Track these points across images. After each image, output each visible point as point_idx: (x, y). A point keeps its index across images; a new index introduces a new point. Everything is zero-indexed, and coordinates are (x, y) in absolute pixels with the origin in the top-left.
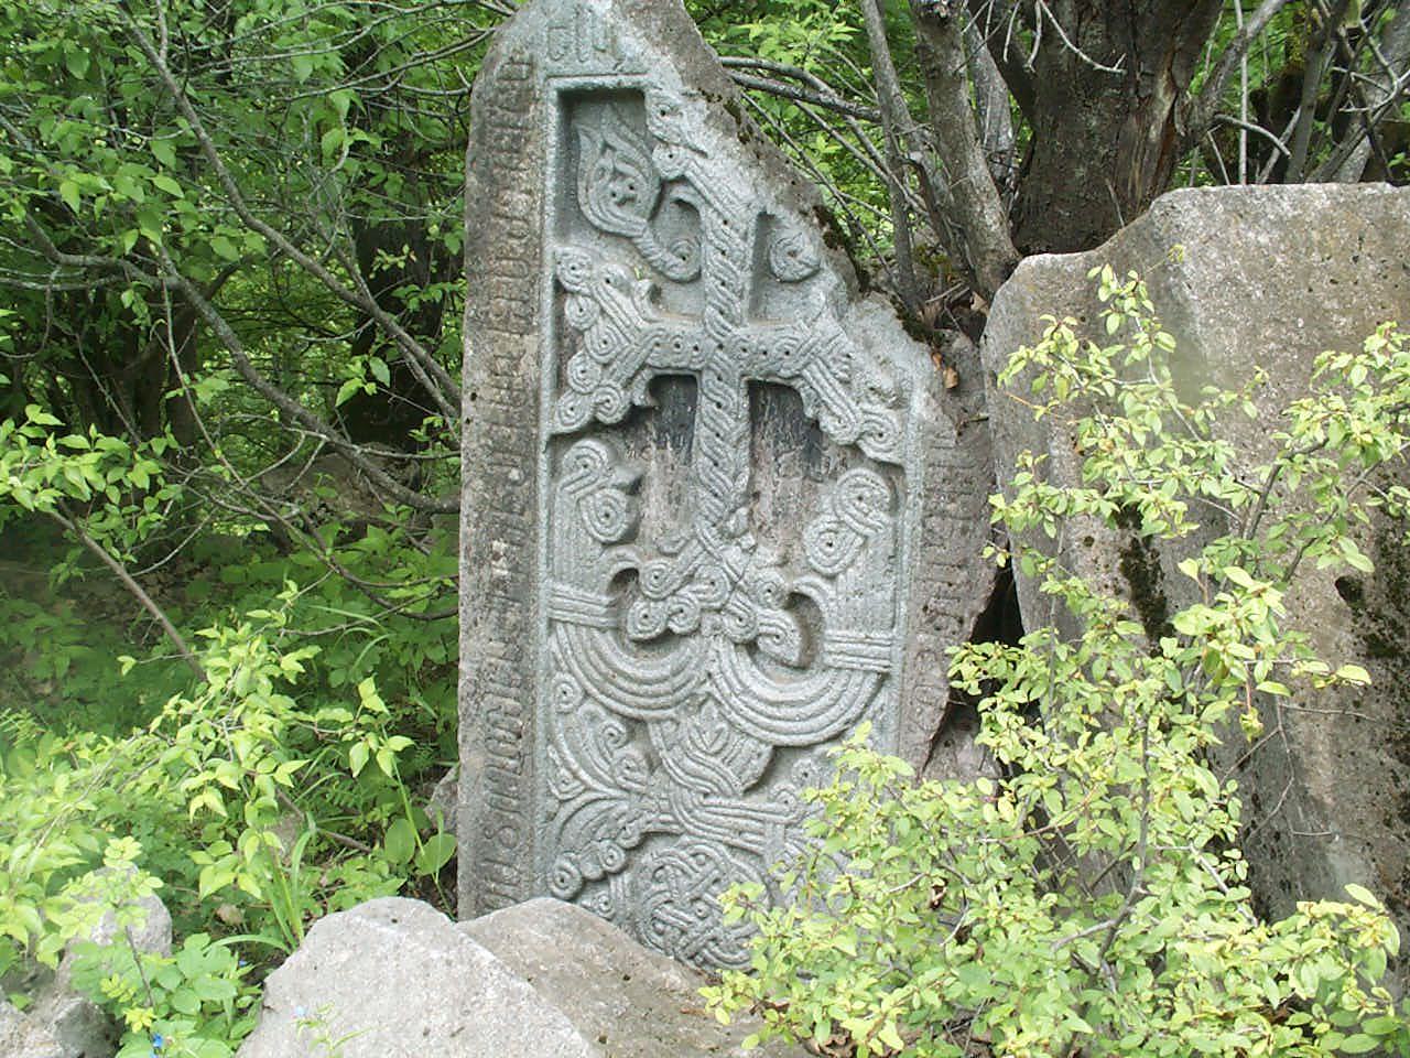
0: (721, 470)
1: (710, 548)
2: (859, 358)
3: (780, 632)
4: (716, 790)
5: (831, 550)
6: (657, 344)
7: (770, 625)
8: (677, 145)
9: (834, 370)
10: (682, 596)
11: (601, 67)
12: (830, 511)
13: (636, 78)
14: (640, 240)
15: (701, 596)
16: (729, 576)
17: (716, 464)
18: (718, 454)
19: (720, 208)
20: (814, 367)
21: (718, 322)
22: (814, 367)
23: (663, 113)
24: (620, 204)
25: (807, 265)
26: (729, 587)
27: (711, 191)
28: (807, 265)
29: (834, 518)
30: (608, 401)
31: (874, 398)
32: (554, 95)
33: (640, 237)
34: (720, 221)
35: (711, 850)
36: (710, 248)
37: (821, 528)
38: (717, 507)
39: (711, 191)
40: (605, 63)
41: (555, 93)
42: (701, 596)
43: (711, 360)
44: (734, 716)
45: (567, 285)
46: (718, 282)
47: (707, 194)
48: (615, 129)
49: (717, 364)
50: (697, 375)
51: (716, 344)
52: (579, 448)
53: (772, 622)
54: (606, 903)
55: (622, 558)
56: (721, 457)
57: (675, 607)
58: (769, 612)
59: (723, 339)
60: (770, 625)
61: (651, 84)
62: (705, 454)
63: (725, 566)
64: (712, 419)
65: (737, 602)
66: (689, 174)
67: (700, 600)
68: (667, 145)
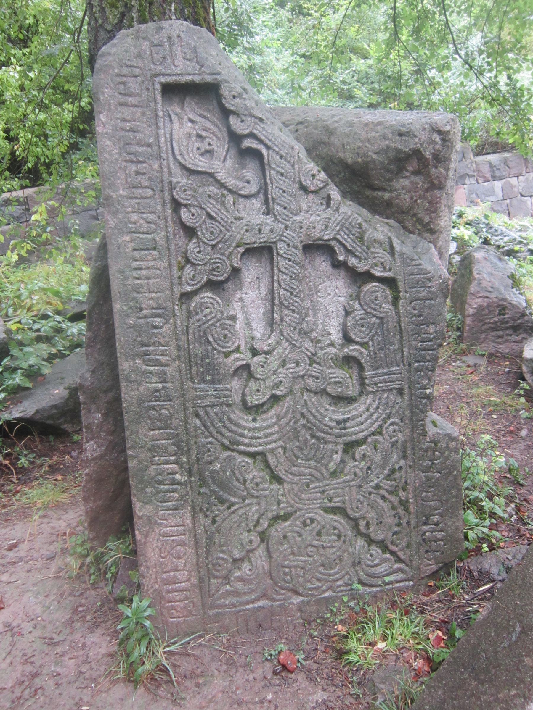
0: (295, 296)
1: (294, 342)
2: (365, 225)
3: (341, 380)
4: (313, 479)
5: (364, 329)
6: (247, 231)
7: (335, 378)
8: (245, 115)
9: (353, 232)
10: (280, 373)
11: (190, 70)
12: (360, 308)
13: (215, 77)
14: (219, 174)
15: (291, 370)
16: (307, 355)
17: (292, 293)
18: (292, 288)
19: (277, 149)
20: (342, 233)
21: (284, 214)
22: (342, 233)
23: (234, 97)
24: (202, 155)
25: (323, 182)
26: (308, 362)
27: (270, 140)
28: (323, 182)
29: (363, 311)
30: (218, 267)
31: (376, 245)
32: (158, 87)
33: (219, 172)
34: (278, 157)
35: (312, 514)
36: (273, 172)
37: (357, 318)
38: (295, 318)
39: (270, 140)
40: (192, 67)
41: (159, 85)
42: (291, 370)
43: (282, 236)
44: (319, 434)
45: (182, 201)
46: (281, 191)
47: (267, 142)
48: (193, 110)
49: (286, 237)
50: (273, 245)
51: (283, 226)
52: (202, 298)
53: (335, 375)
54: (250, 570)
55: (237, 359)
56: (295, 289)
57: (277, 380)
58: (331, 371)
59: (288, 223)
60: (335, 378)
61: (224, 80)
62: (284, 289)
63: (304, 349)
64: (286, 268)
65: (315, 370)
66: (255, 131)
67: (292, 373)
68: (238, 115)
